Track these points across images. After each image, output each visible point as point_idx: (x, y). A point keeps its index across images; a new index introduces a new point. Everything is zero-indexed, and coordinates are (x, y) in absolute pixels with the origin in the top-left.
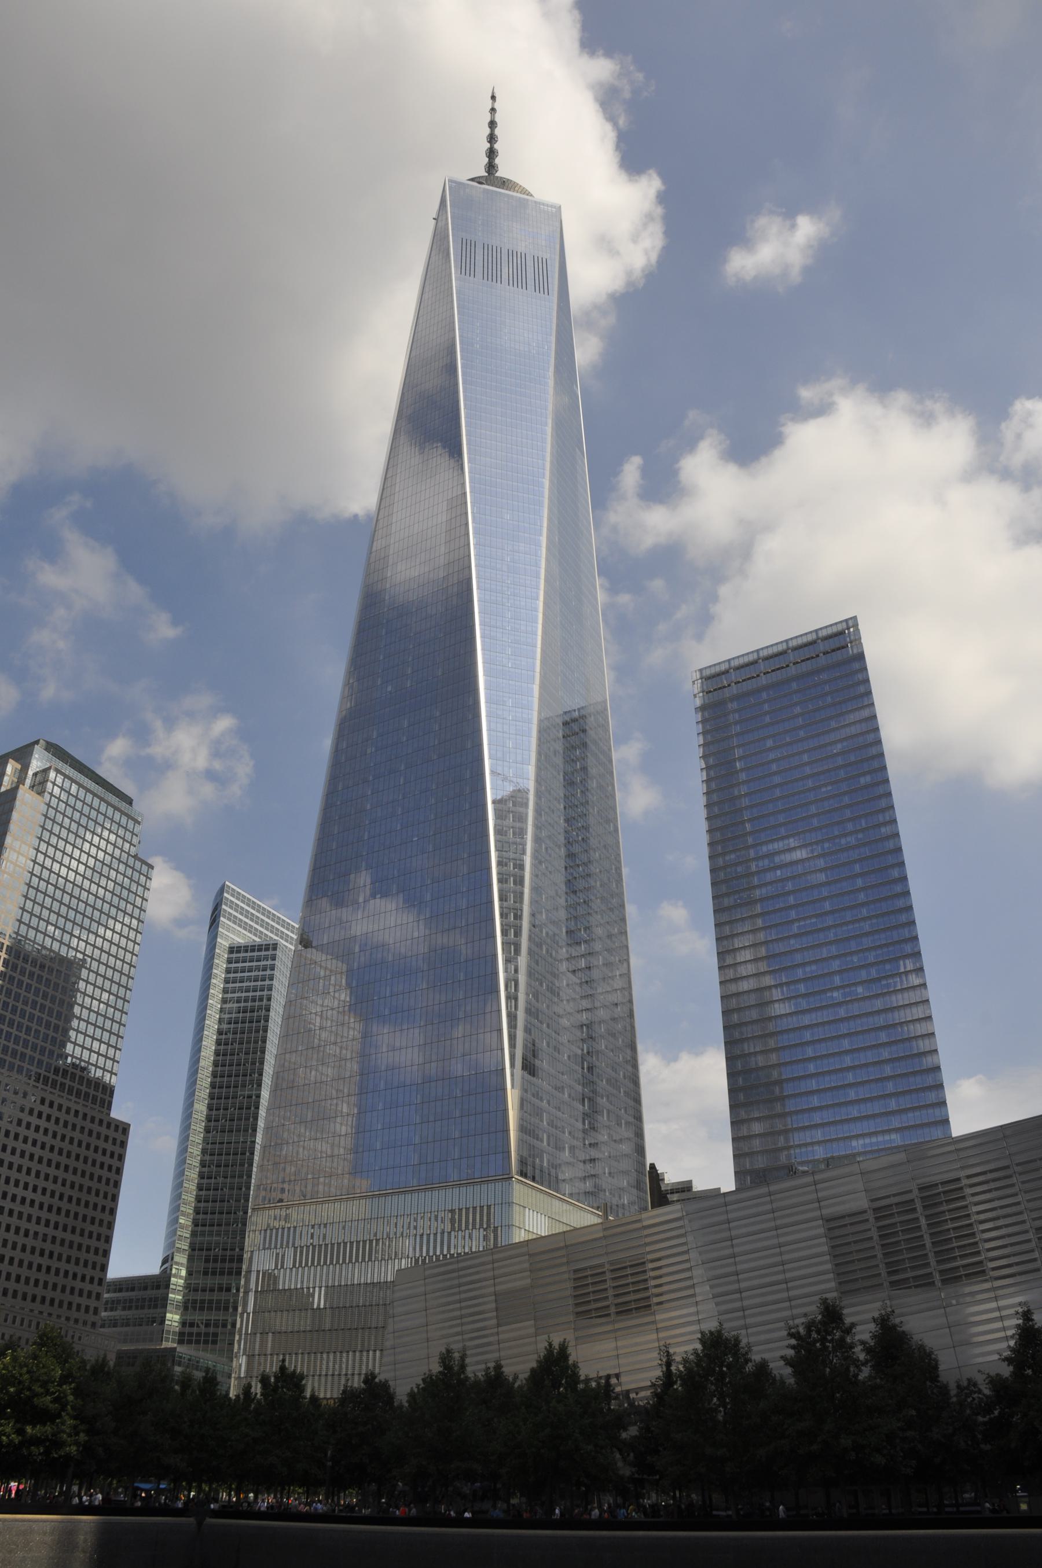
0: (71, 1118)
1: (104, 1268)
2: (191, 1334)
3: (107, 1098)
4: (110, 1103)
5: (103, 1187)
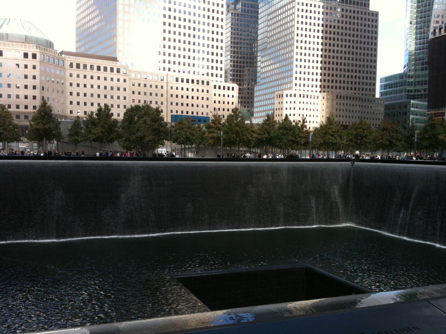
0: (352, 14)
2: (418, 95)
4: (369, 4)
5: (370, 40)
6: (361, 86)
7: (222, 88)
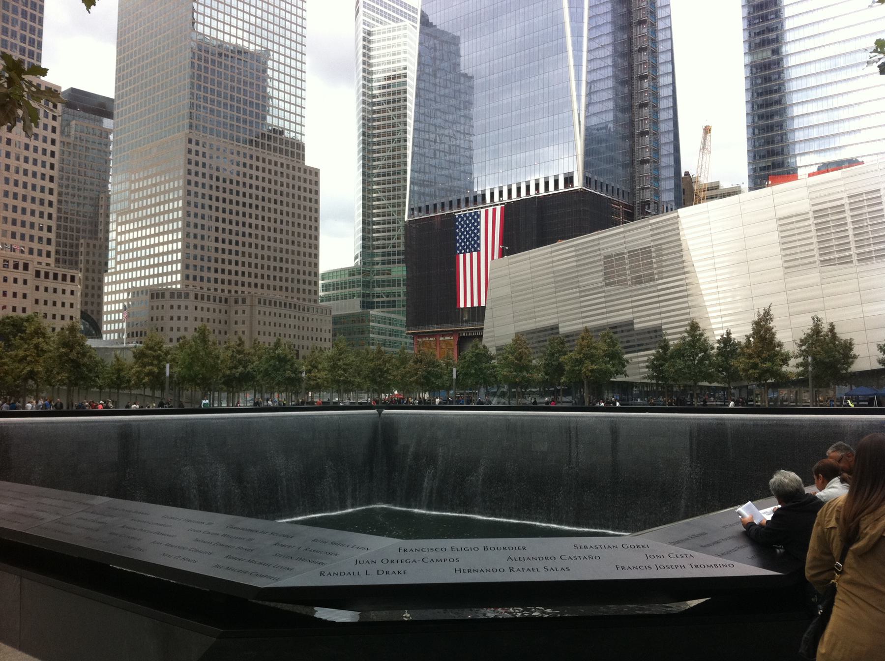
0: (279, 169)
1: (316, 265)
3: (301, 152)
4: (303, 155)
6: (296, 285)
7: (51, 276)
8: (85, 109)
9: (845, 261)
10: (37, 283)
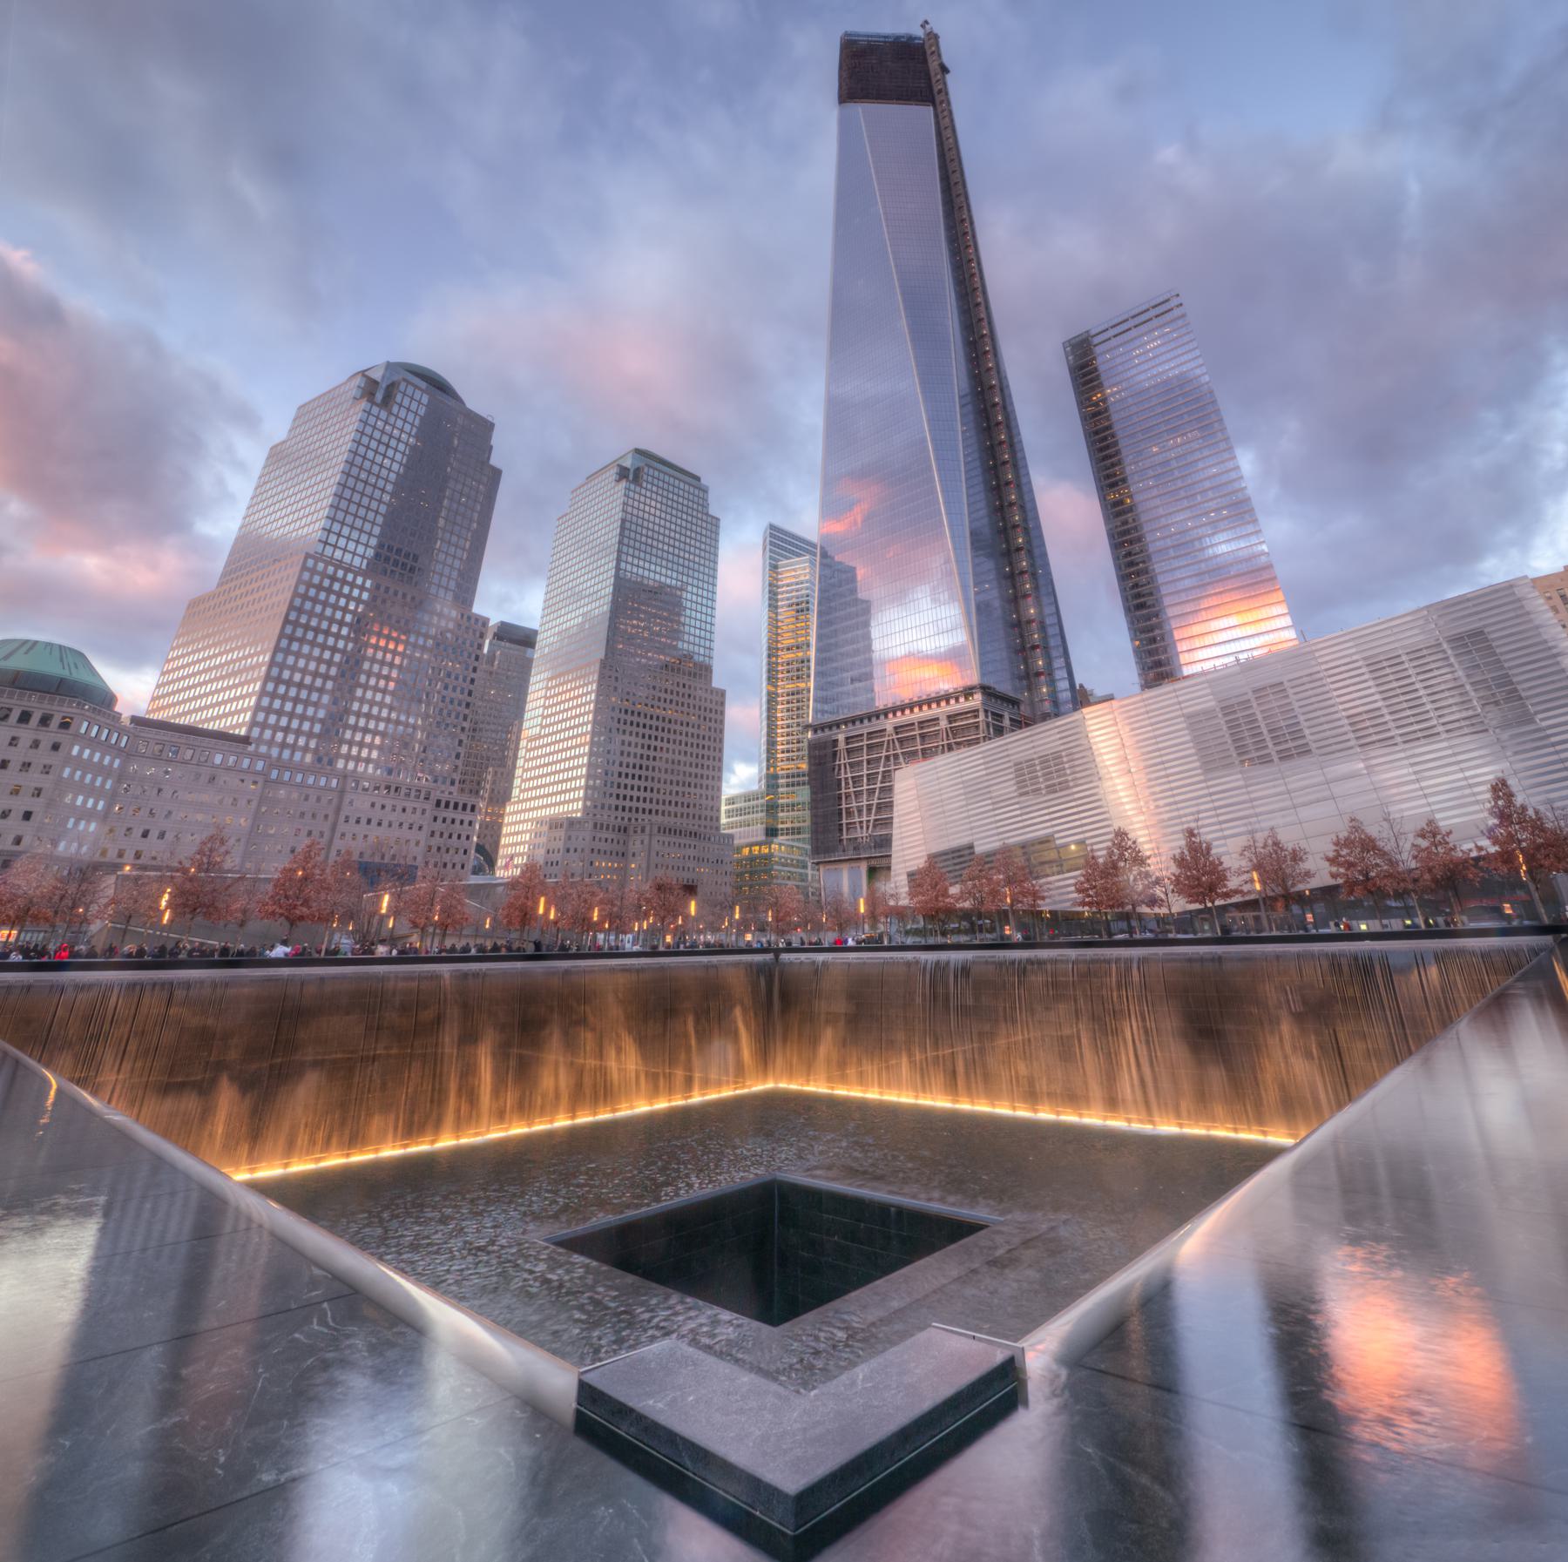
5: (713, 735)
8: (511, 641)
9: (1265, 760)
10: (436, 813)
